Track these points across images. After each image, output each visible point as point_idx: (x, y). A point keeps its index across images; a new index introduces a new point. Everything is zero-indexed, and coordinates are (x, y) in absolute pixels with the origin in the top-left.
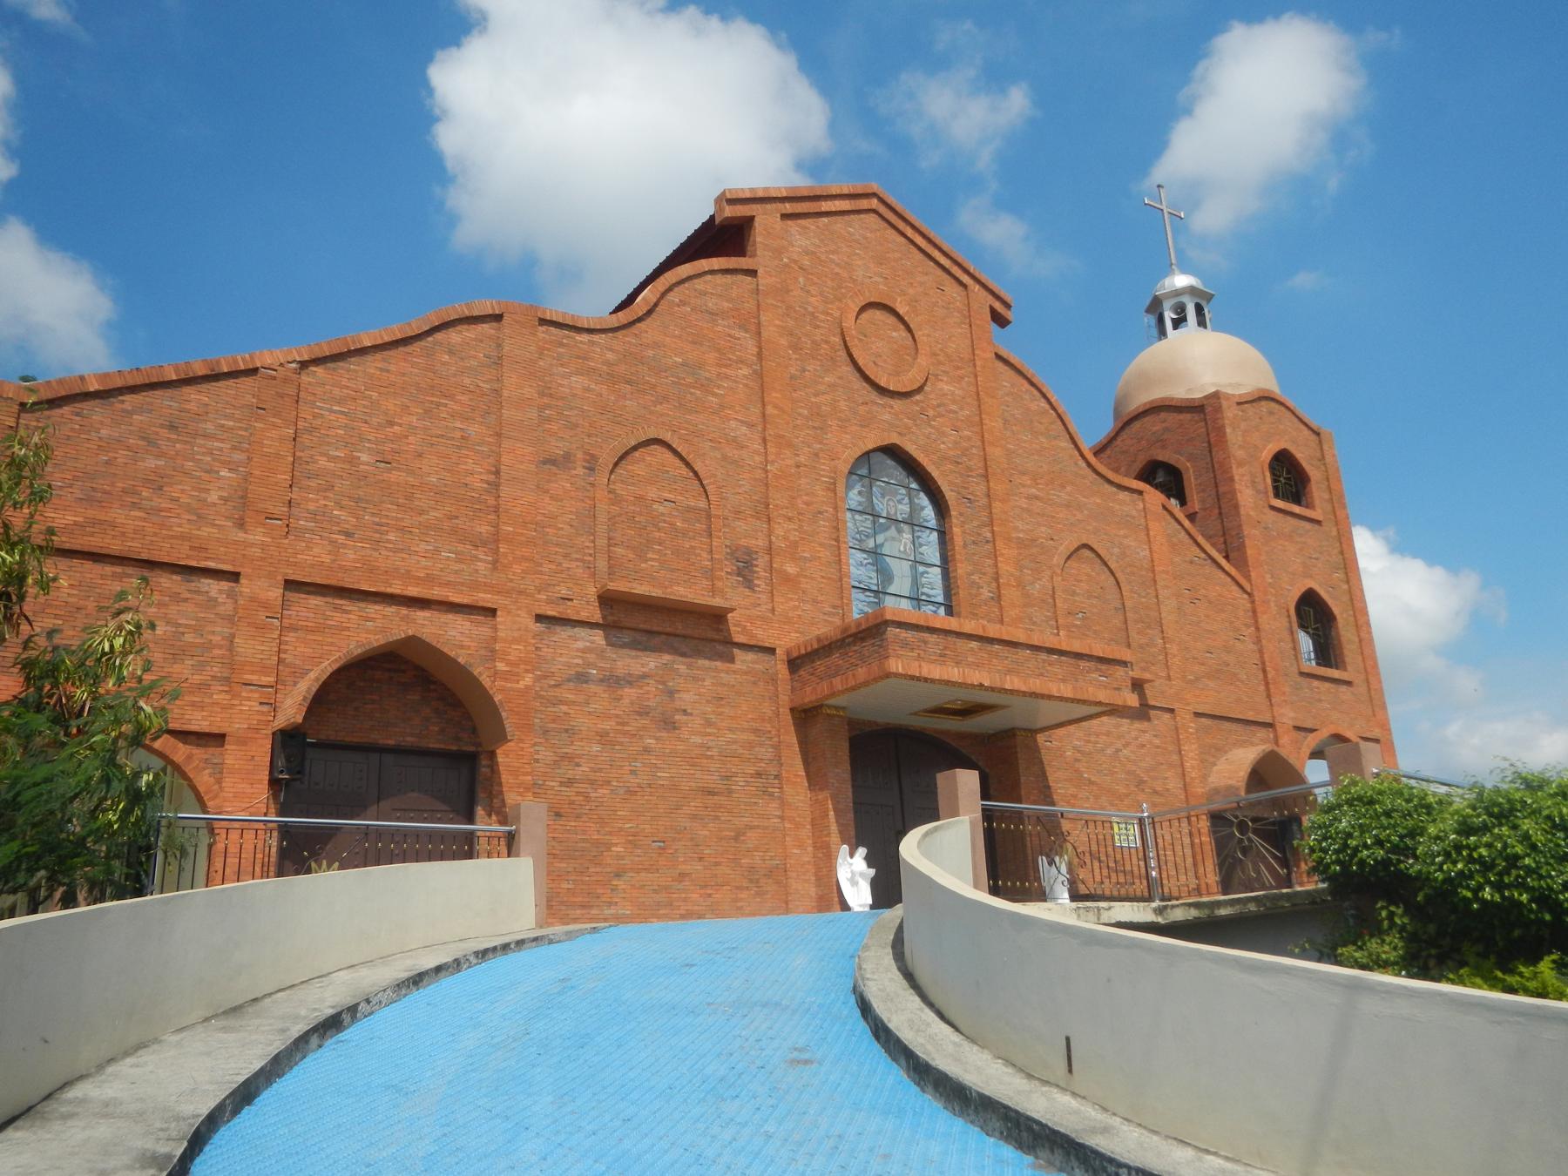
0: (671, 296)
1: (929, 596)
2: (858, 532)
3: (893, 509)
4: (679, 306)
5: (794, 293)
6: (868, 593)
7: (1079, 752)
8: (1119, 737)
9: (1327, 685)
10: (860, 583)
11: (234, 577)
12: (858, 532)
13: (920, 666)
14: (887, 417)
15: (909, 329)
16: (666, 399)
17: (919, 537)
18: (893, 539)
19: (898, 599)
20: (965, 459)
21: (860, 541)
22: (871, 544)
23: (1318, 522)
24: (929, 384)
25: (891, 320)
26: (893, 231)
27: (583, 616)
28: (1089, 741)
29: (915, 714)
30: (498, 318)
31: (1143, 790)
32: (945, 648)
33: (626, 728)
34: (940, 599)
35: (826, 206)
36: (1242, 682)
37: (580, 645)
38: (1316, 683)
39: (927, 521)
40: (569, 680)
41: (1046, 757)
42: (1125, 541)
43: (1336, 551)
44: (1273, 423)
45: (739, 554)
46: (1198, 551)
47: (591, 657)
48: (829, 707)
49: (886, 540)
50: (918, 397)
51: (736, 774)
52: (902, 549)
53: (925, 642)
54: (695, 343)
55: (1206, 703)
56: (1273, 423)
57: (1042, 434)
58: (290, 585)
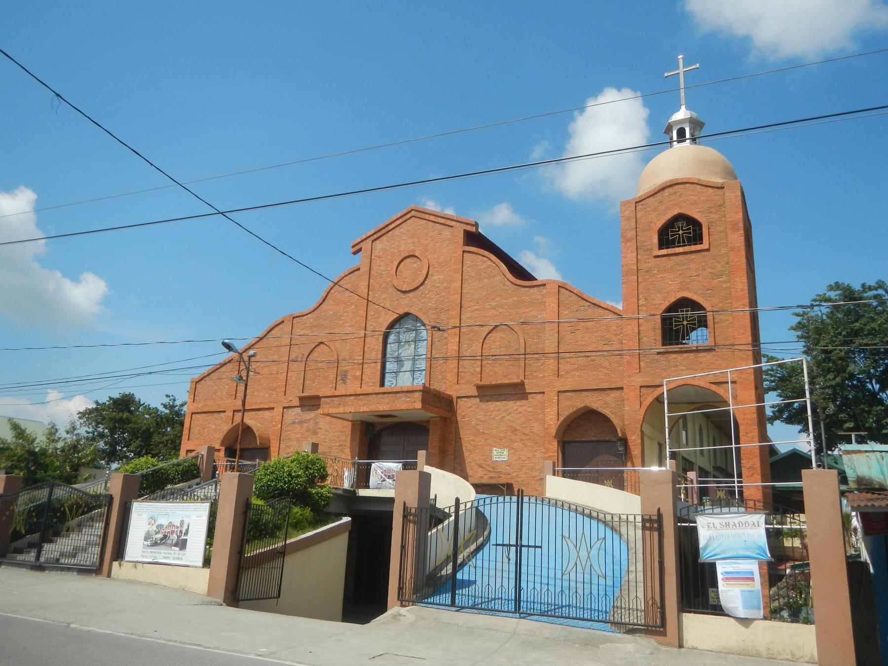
0: (332, 291)
4: (334, 293)
5: (375, 269)
7: (480, 421)
8: (505, 411)
9: (685, 355)
11: (224, 412)
12: (392, 351)
13: (329, 410)
14: (406, 302)
15: (421, 260)
16: (326, 328)
18: (406, 349)
20: (440, 305)
22: (397, 354)
23: (708, 250)
24: (428, 280)
25: (414, 259)
26: (421, 220)
27: (295, 405)
28: (487, 415)
30: (283, 322)
31: (516, 434)
32: (341, 402)
33: (304, 436)
35: (391, 227)
36: (604, 368)
37: (294, 413)
38: (673, 356)
39: (422, 337)
40: (291, 424)
41: (460, 426)
42: (532, 313)
43: (723, 263)
44: (673, 200)
45: (343, 373)
46: (584, 302)
47: (296, 416)
49: (403, 351)
50: (421, 288)
51: (333, 446)
53: (334, 401)
54: (337, 304)
55: (570, 385)
56: (673, 200)
57: (485, 278)
58: (234, 411)
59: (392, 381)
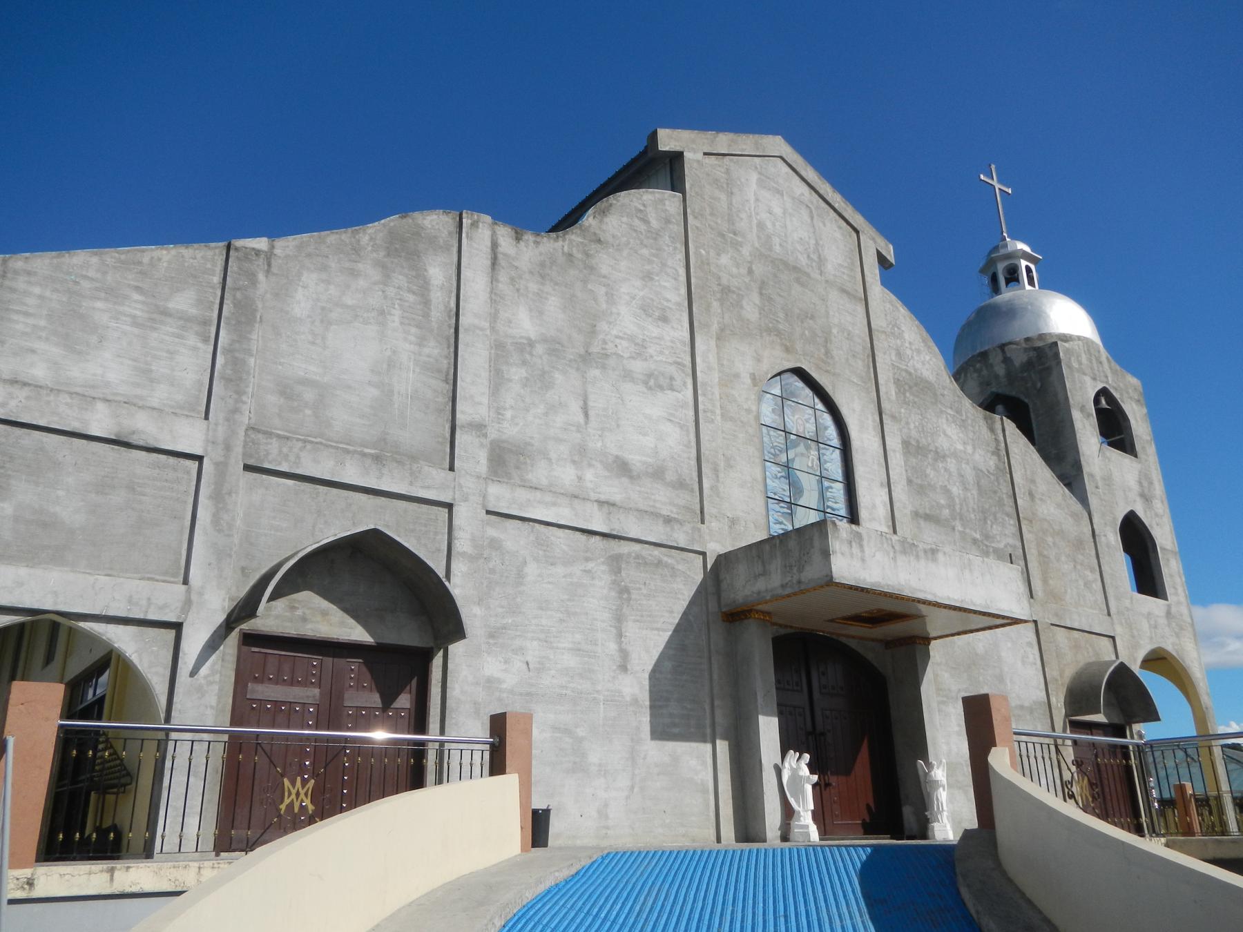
1: (833, 509)
2: (773, 447)
3: (802, 427)
6: (782, 505)
10: (775, 494)
12: (773, 447)
17: (824, 454)
18: (802, 455)
19: (807, 509)
21: (775, 455)
22: (783, 458)
29: (832, 621)
34: (843, 512)
48: (757, 611)
49: (796, 456)
52: (810, 465)
59: (781, 523)
